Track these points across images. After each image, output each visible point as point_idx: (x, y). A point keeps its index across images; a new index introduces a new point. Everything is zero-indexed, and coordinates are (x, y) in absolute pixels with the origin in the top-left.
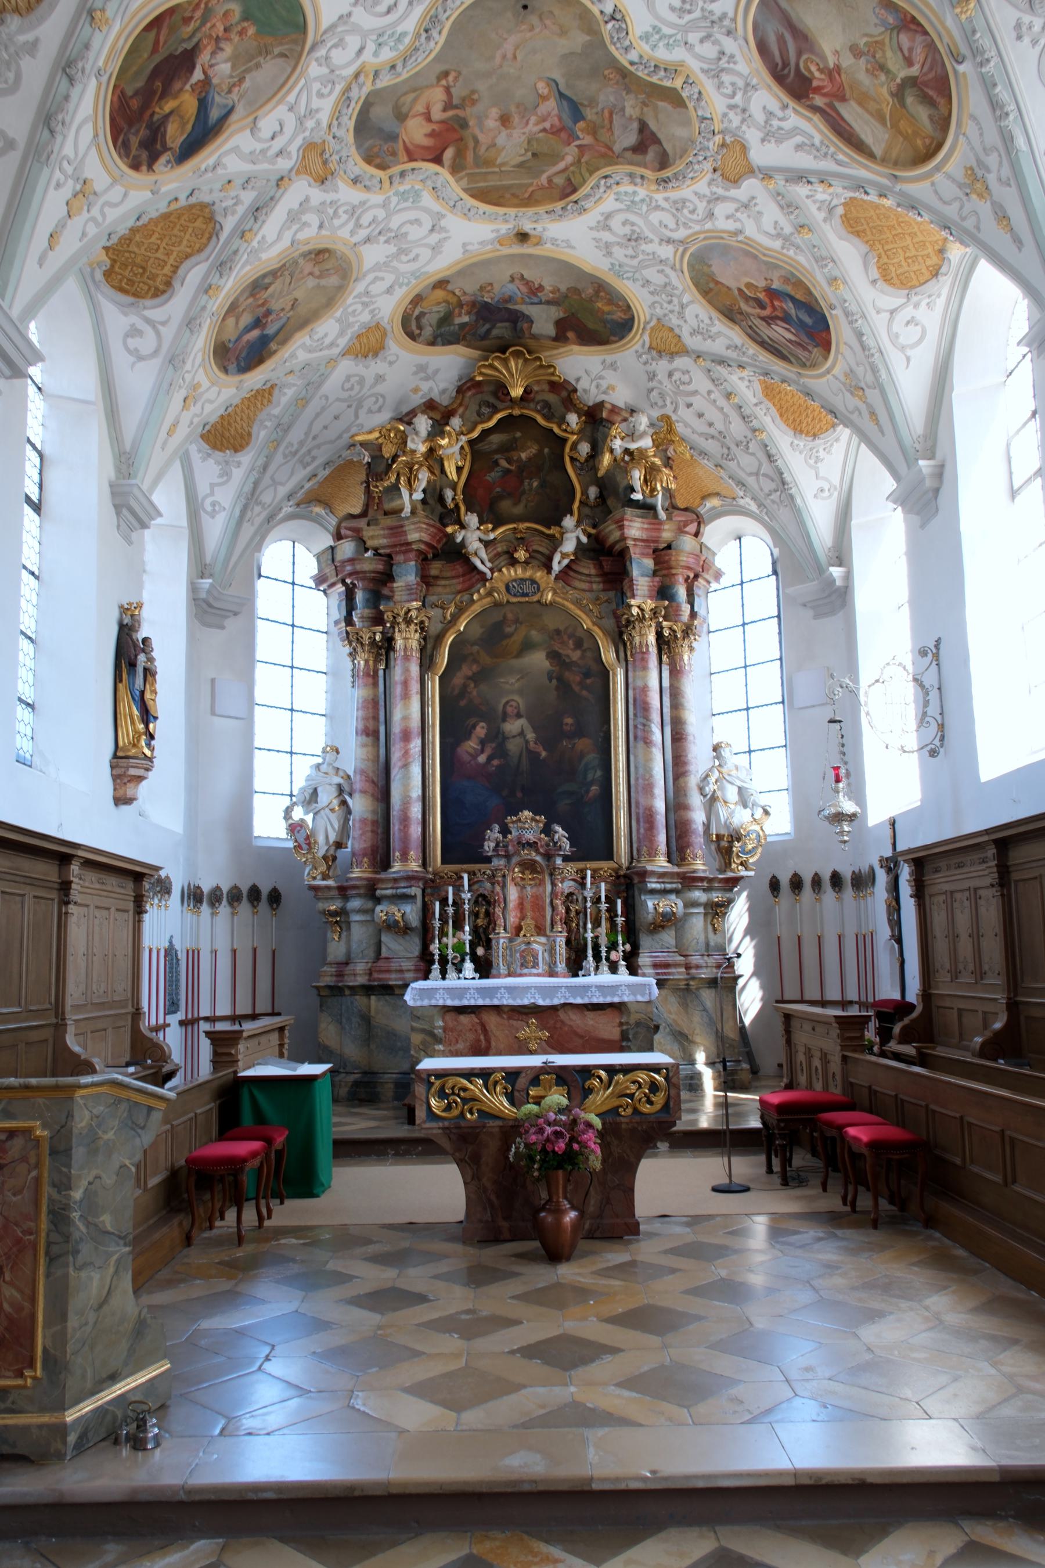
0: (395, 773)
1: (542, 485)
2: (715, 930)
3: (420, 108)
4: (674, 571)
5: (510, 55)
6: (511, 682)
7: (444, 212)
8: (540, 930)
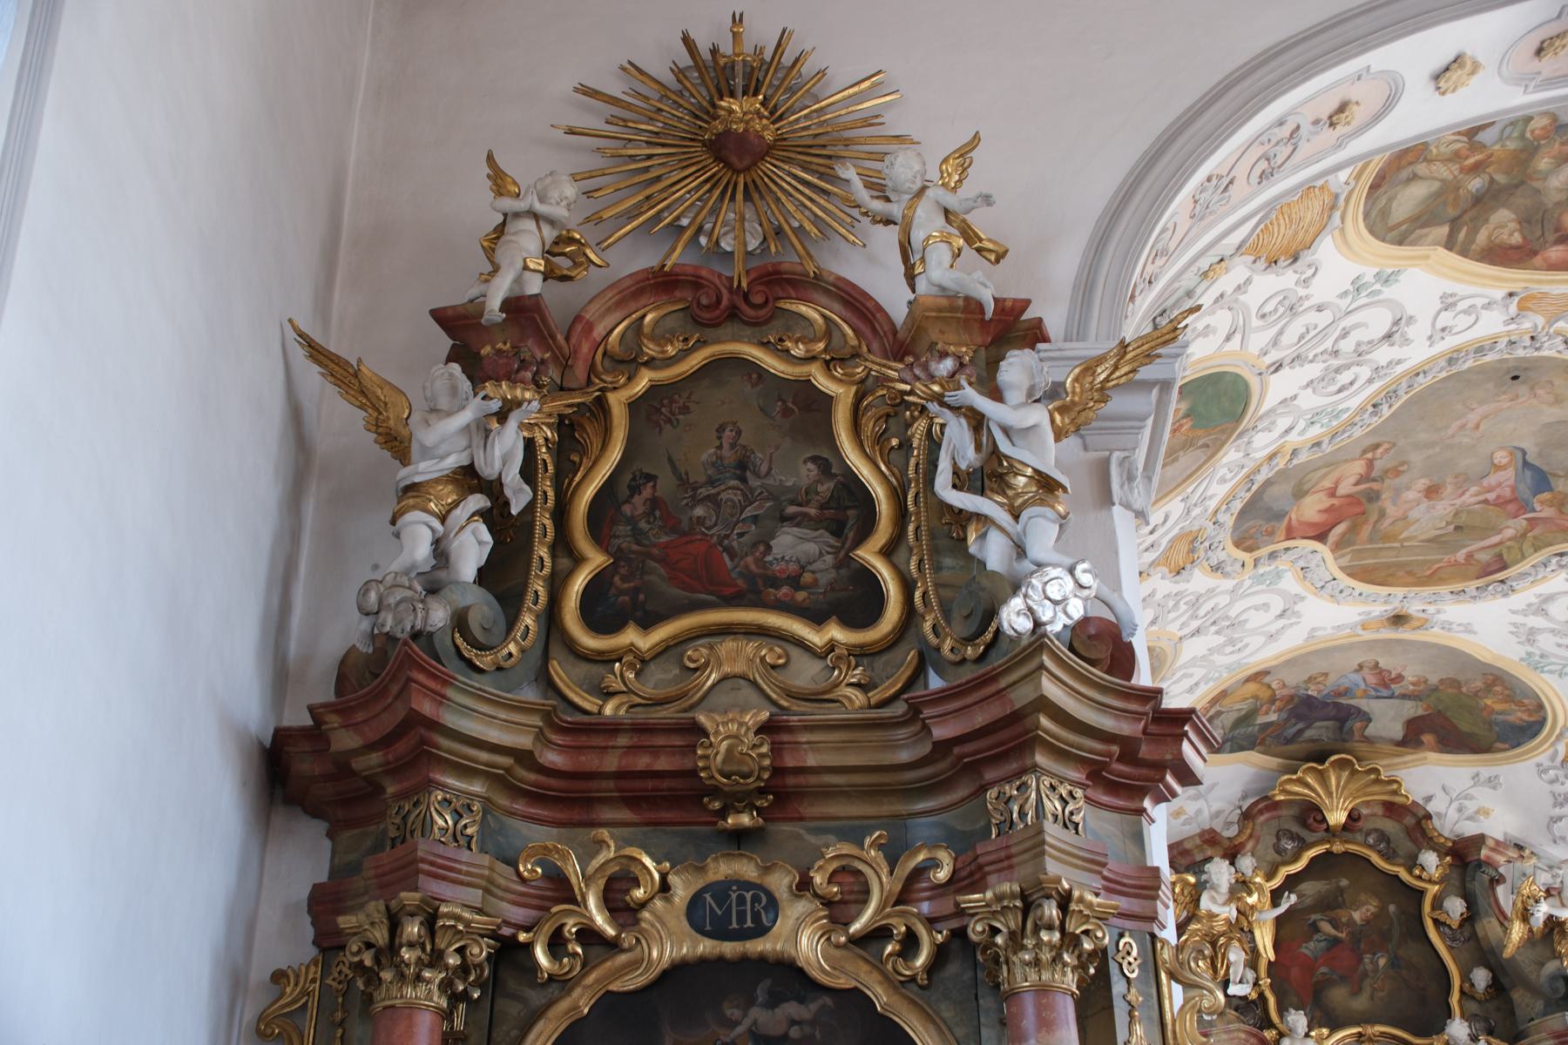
1: (1394, 963)
3: (1327, 483)
5: (1471, 425)
7: (1304, 594)
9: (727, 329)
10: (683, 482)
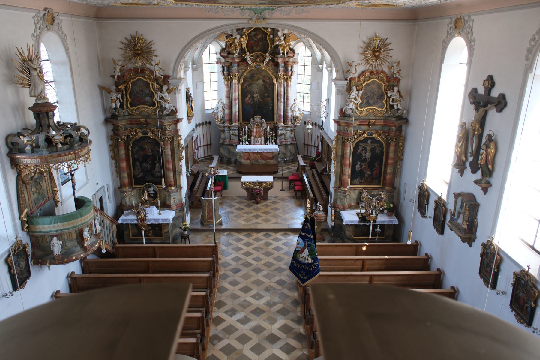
0: (233, 106)
6: (255, 86)
8: (260, 137)
9: (140, 75)
10: (137, 92)
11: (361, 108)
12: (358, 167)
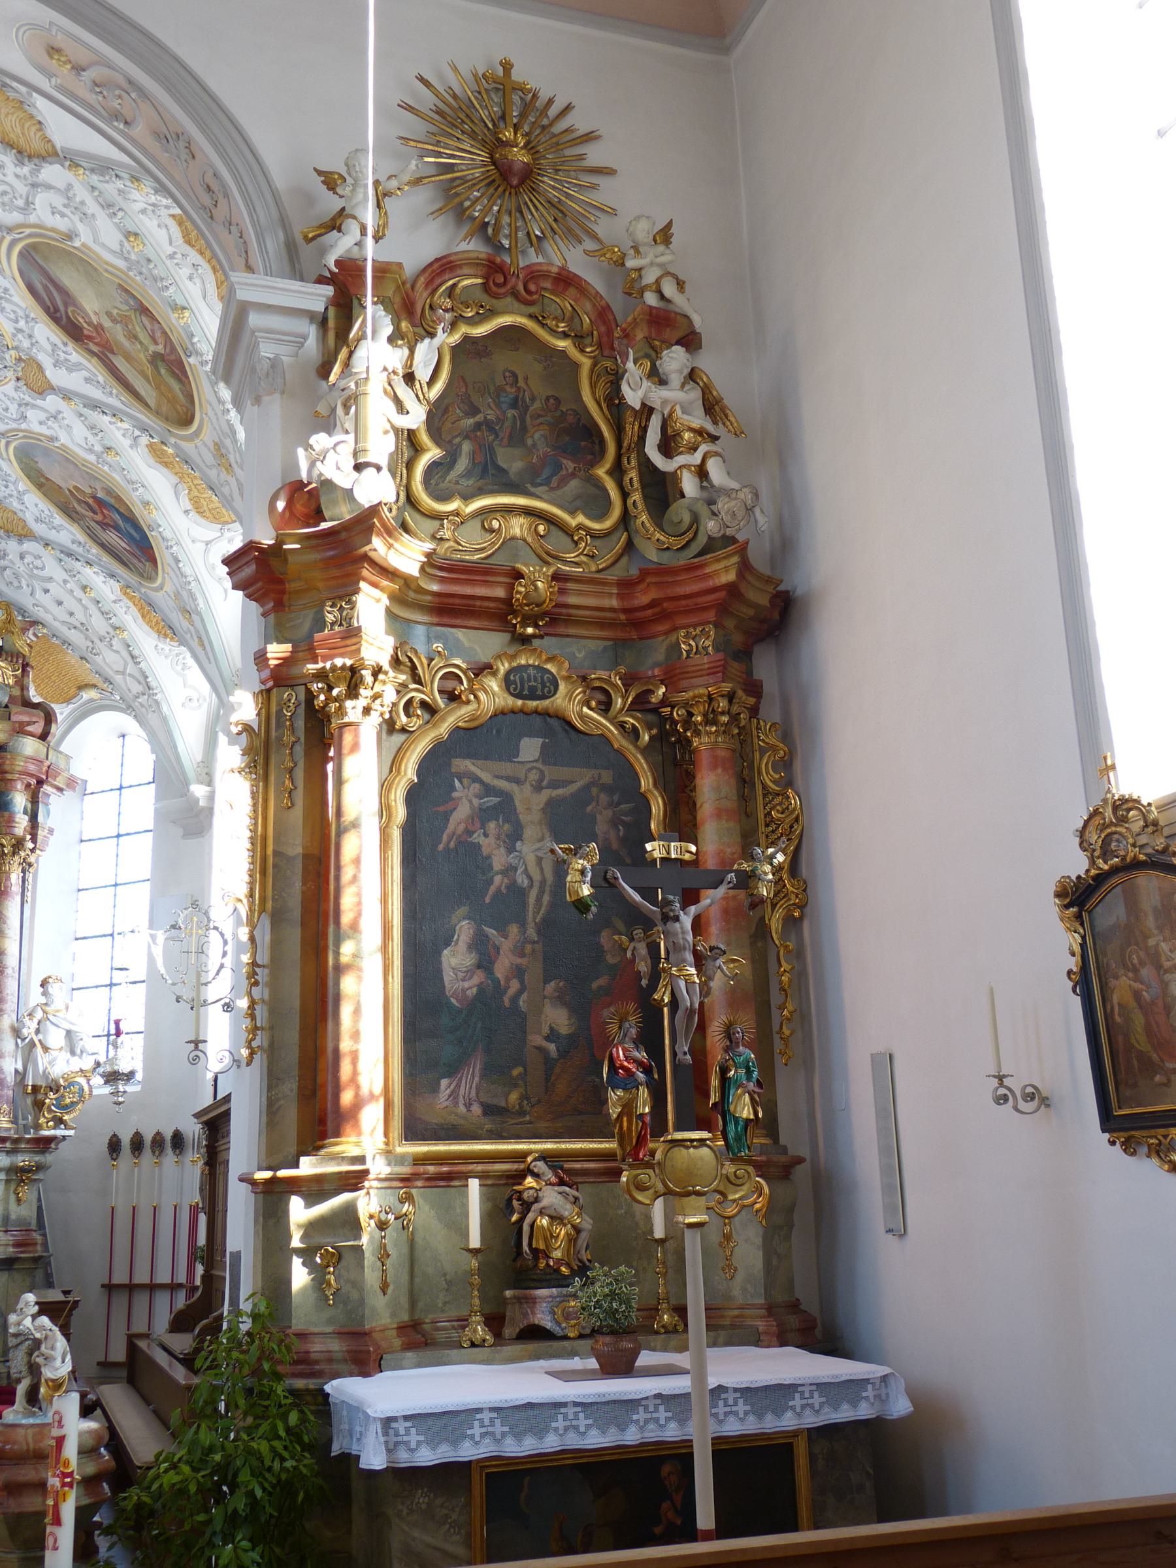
2: (19, 1200)
4: (9, 776)
11: (443, 498)
12: (456, 961)
